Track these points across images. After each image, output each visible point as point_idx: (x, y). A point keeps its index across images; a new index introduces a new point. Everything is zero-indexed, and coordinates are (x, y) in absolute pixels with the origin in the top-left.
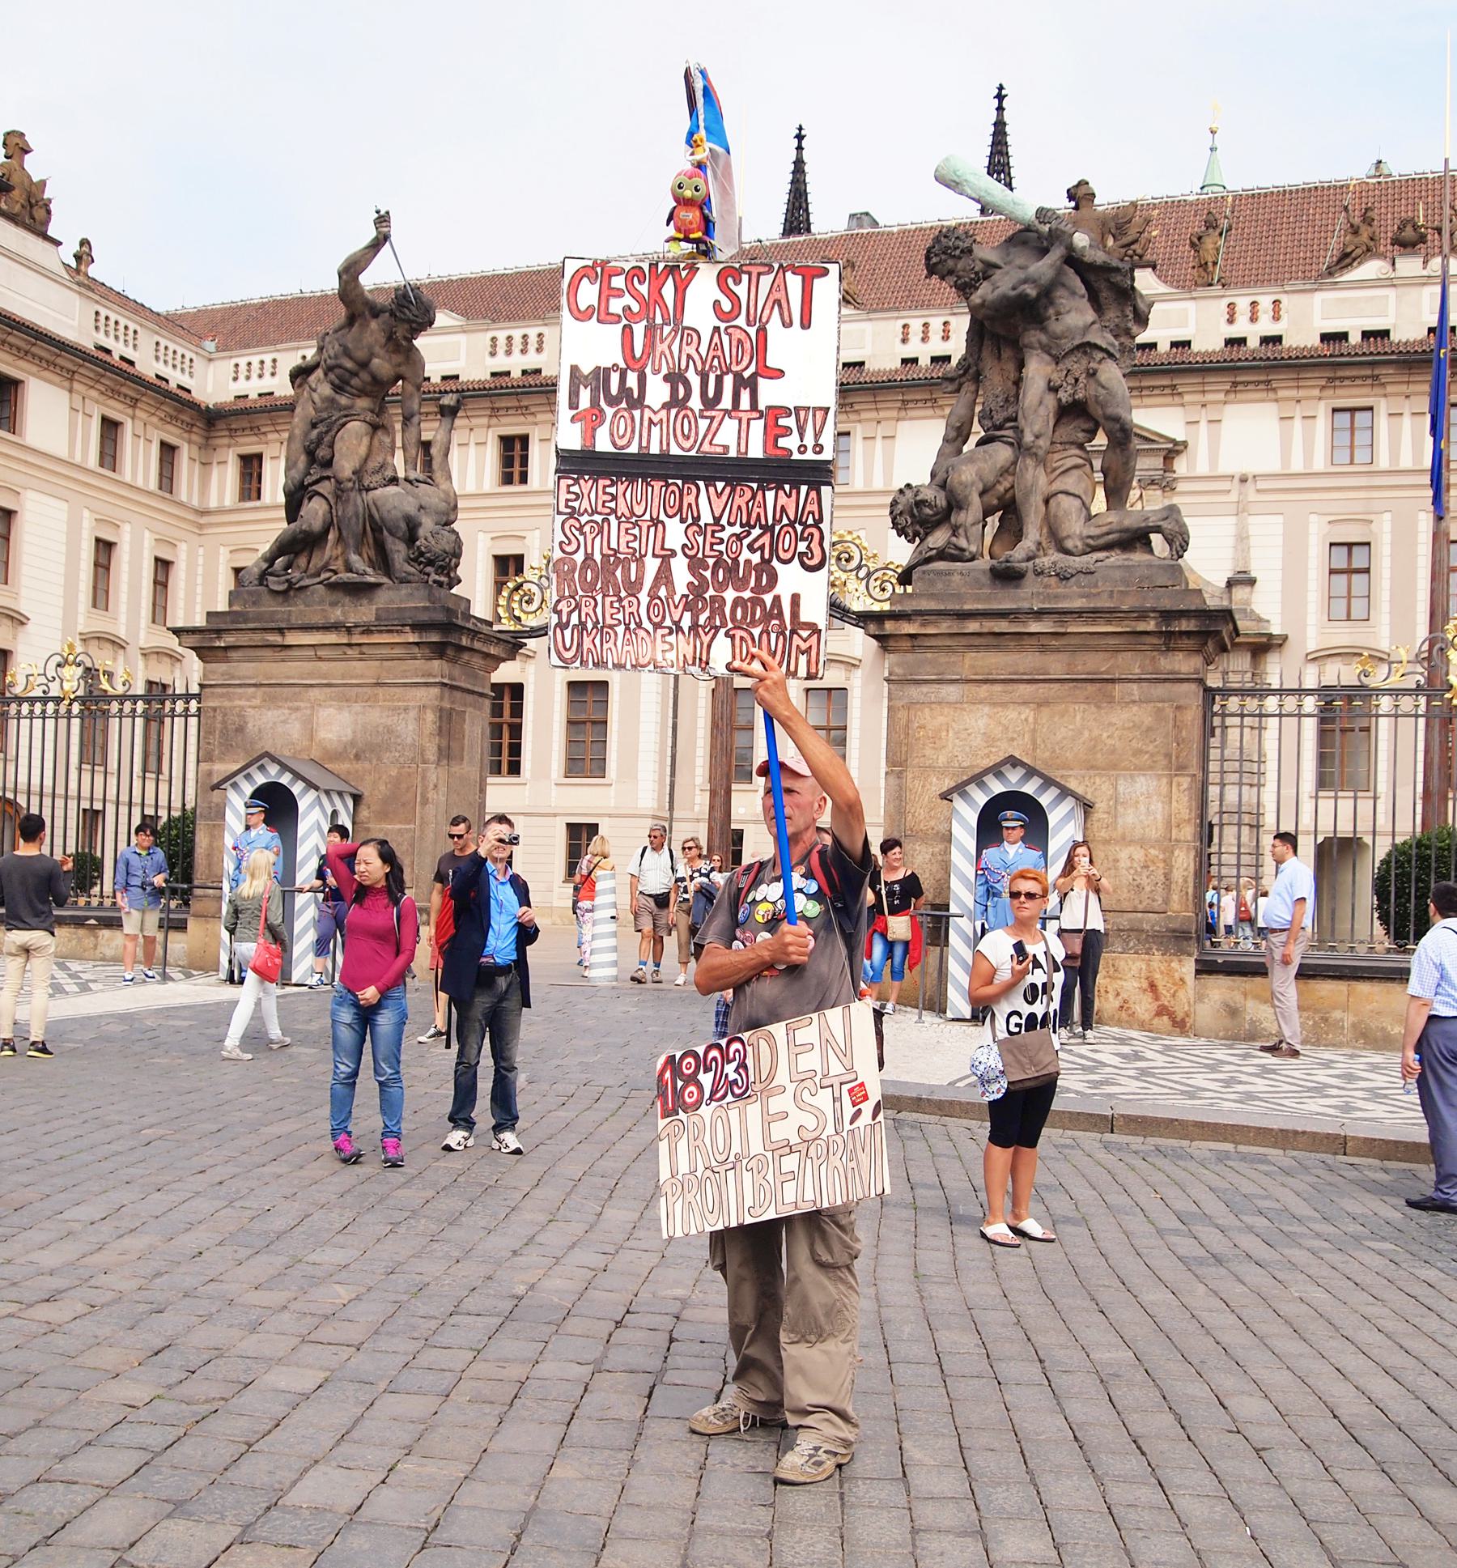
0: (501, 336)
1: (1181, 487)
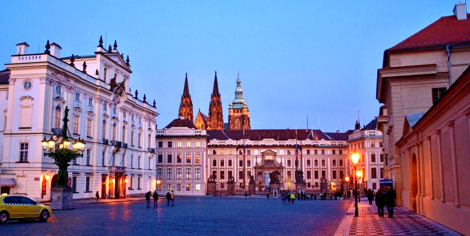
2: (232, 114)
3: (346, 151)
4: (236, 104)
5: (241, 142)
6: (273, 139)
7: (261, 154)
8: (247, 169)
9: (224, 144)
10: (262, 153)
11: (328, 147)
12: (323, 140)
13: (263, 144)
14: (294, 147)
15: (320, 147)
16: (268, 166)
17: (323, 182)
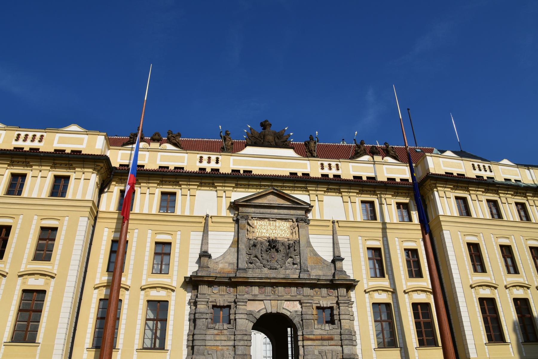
0: (23, 134)
1: (312, 223)
6: (290, 152)
9: (36, 144)
10: (235, 206)
13: (242, 168)
14: (391, 186)
16: (266, 270)
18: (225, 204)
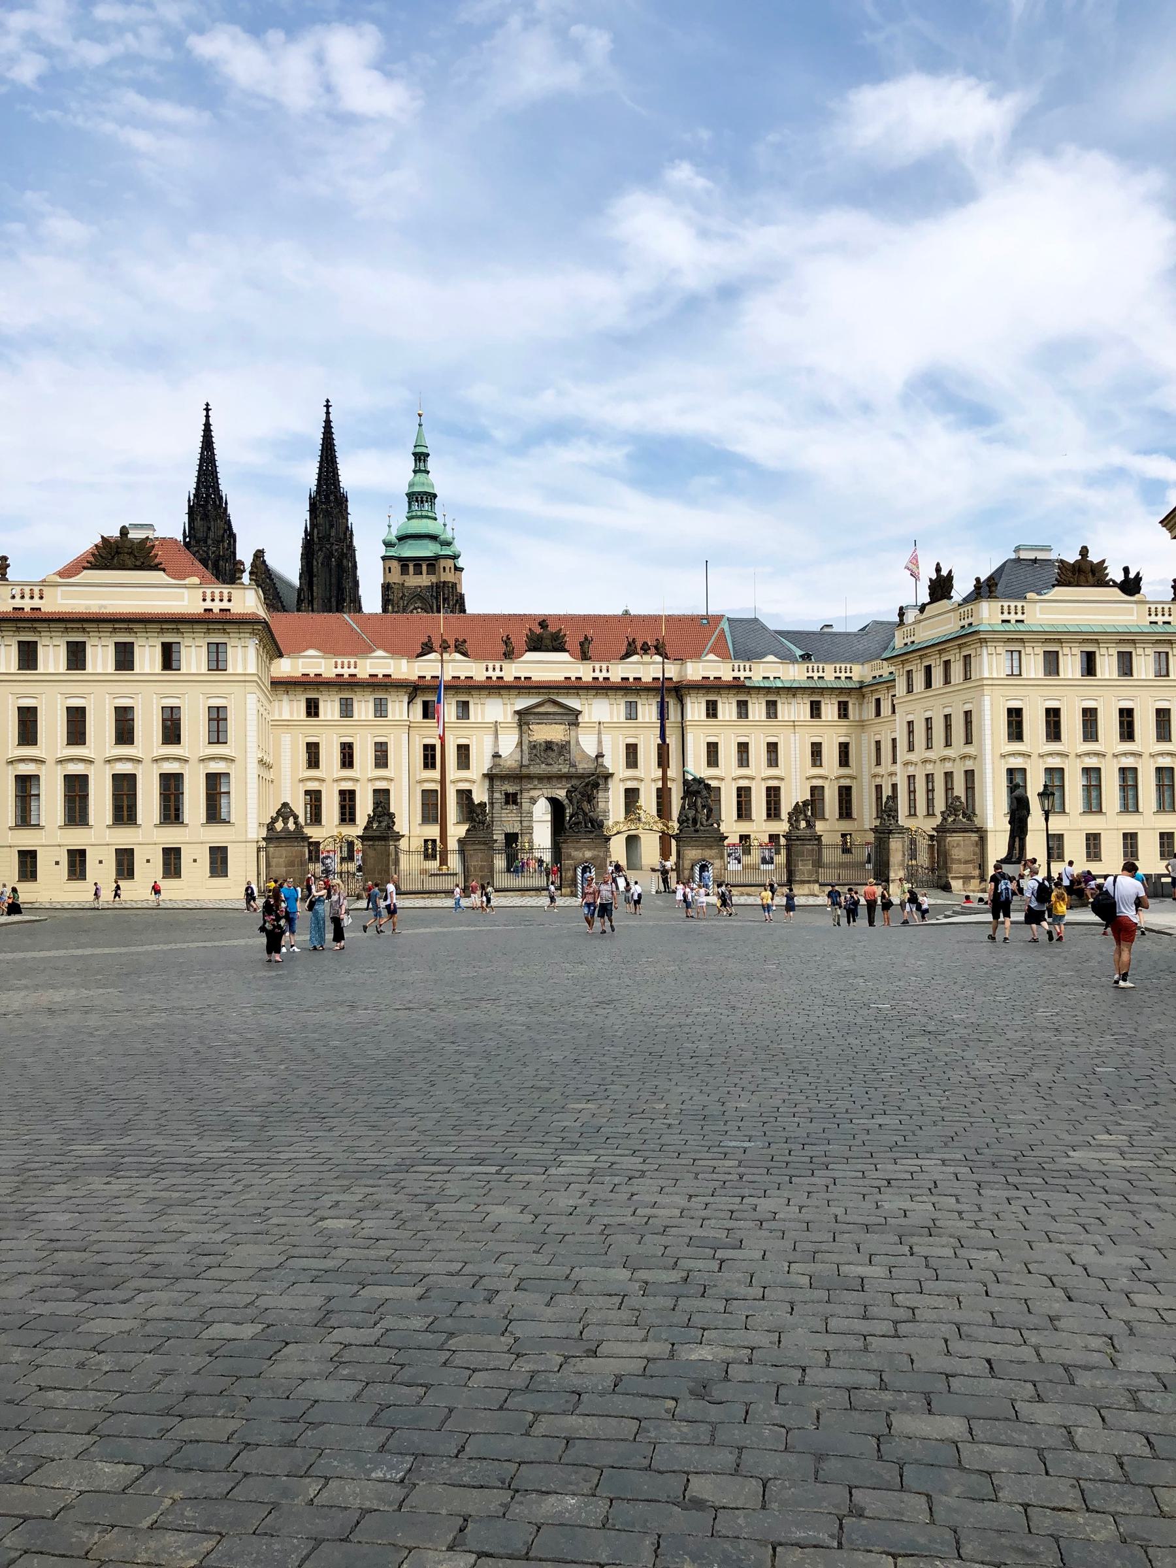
0: (339, 661)
2: (396, 577)
3: (865, 706)
4: (410, 542)
5: (427, 667)
6: (564, 656)
7: (517, 717)
8: (453, 782)
9: (352, 671)
10: (518, 713)
11: (792, 691)
12: (771, 658)
13: (523, 675)
15: (759, 689)
17: (799, 833)
18: (510, 710)
